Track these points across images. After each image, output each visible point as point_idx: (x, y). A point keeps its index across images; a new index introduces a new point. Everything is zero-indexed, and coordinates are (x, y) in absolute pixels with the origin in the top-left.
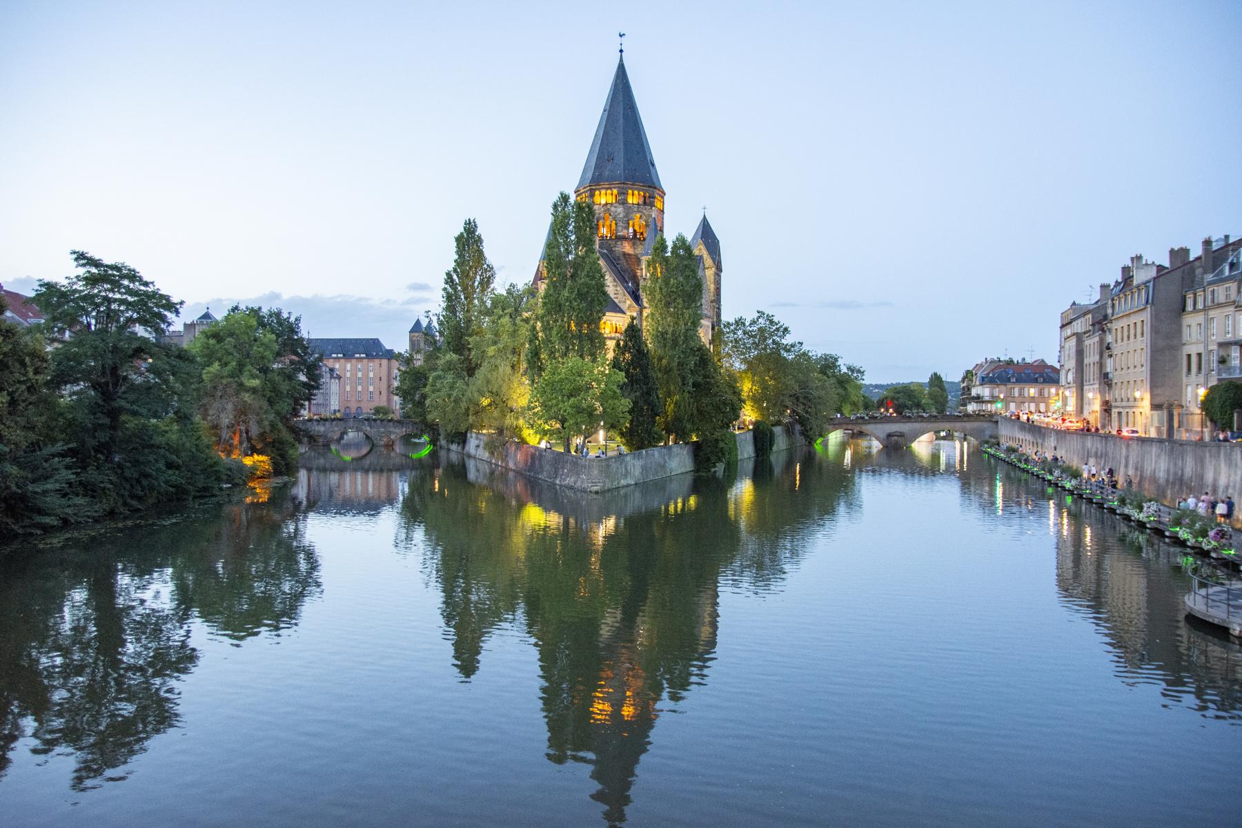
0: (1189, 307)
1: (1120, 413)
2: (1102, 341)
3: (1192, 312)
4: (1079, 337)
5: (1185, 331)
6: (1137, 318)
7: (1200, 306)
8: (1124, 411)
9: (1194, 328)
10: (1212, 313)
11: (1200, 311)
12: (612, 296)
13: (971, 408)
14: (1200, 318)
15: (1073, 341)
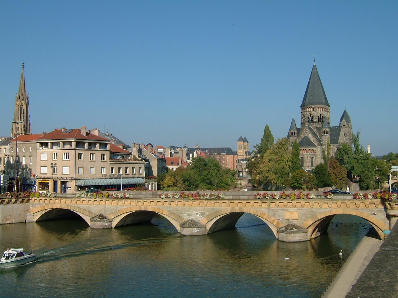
12: (312, 141)
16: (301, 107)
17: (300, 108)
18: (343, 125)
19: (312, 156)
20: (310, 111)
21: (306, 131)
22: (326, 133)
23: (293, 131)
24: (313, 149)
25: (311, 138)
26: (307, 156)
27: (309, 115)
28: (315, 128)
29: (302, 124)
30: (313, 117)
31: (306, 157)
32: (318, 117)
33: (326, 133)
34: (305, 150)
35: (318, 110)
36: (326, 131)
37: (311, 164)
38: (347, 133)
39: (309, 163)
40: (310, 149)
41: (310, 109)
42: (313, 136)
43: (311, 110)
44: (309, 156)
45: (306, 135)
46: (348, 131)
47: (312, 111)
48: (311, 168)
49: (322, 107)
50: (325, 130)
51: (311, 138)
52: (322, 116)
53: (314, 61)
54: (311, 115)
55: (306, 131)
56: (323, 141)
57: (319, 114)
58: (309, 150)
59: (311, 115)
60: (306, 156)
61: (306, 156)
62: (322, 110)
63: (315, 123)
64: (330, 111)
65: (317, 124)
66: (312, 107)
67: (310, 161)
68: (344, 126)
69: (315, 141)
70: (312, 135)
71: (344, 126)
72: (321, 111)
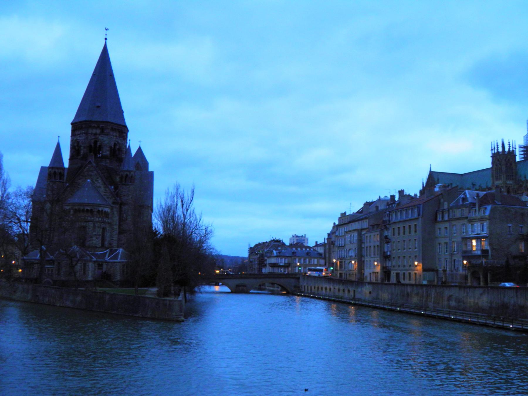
0: (439, 218)
1: (398, 274)
2: (381, 235)
3: (441, 222)
4: (360, 231)
5: (438, 232)
6: (413, 224)
7: (446, 218)
8: (401, 273)
9: (443, 229)
10: (454, 223)
11: (446, 221)
12: (102, 194)
13: (266, 270)
14: (447, 225)
15: (356, 234)
16: (72, 124)
17: (70, 126)
19: (103, 225)
20: (95, 134)
21: (90, 173)
23: (57, 171)
25: (100, 187)
26: (94, 224)
27: (93, 141)
29: (71, 159)
30: (100, 146)
31: (92, 225)
32: (111, 147)
34: (91, 210)
37: (100, 242)
39: (97, 238)
40: (100, 209)
41: (96, 128)
42: (105, 184)
43: (98, 131)
44: (97, 225)
48: (100, 249)
51: (100, 187)
52: (117, 147)
53: (106, 39)
54: (95, 143)
55: (90, 173)
56: (124, 196)
57: (113, 143)
58: (99, 210)
59: (95, 143)
60: (91, 225)
61: (91, 225)
62: (118, 135)
67: (99, 235)
70: (102, 180)
72: (116, 136)
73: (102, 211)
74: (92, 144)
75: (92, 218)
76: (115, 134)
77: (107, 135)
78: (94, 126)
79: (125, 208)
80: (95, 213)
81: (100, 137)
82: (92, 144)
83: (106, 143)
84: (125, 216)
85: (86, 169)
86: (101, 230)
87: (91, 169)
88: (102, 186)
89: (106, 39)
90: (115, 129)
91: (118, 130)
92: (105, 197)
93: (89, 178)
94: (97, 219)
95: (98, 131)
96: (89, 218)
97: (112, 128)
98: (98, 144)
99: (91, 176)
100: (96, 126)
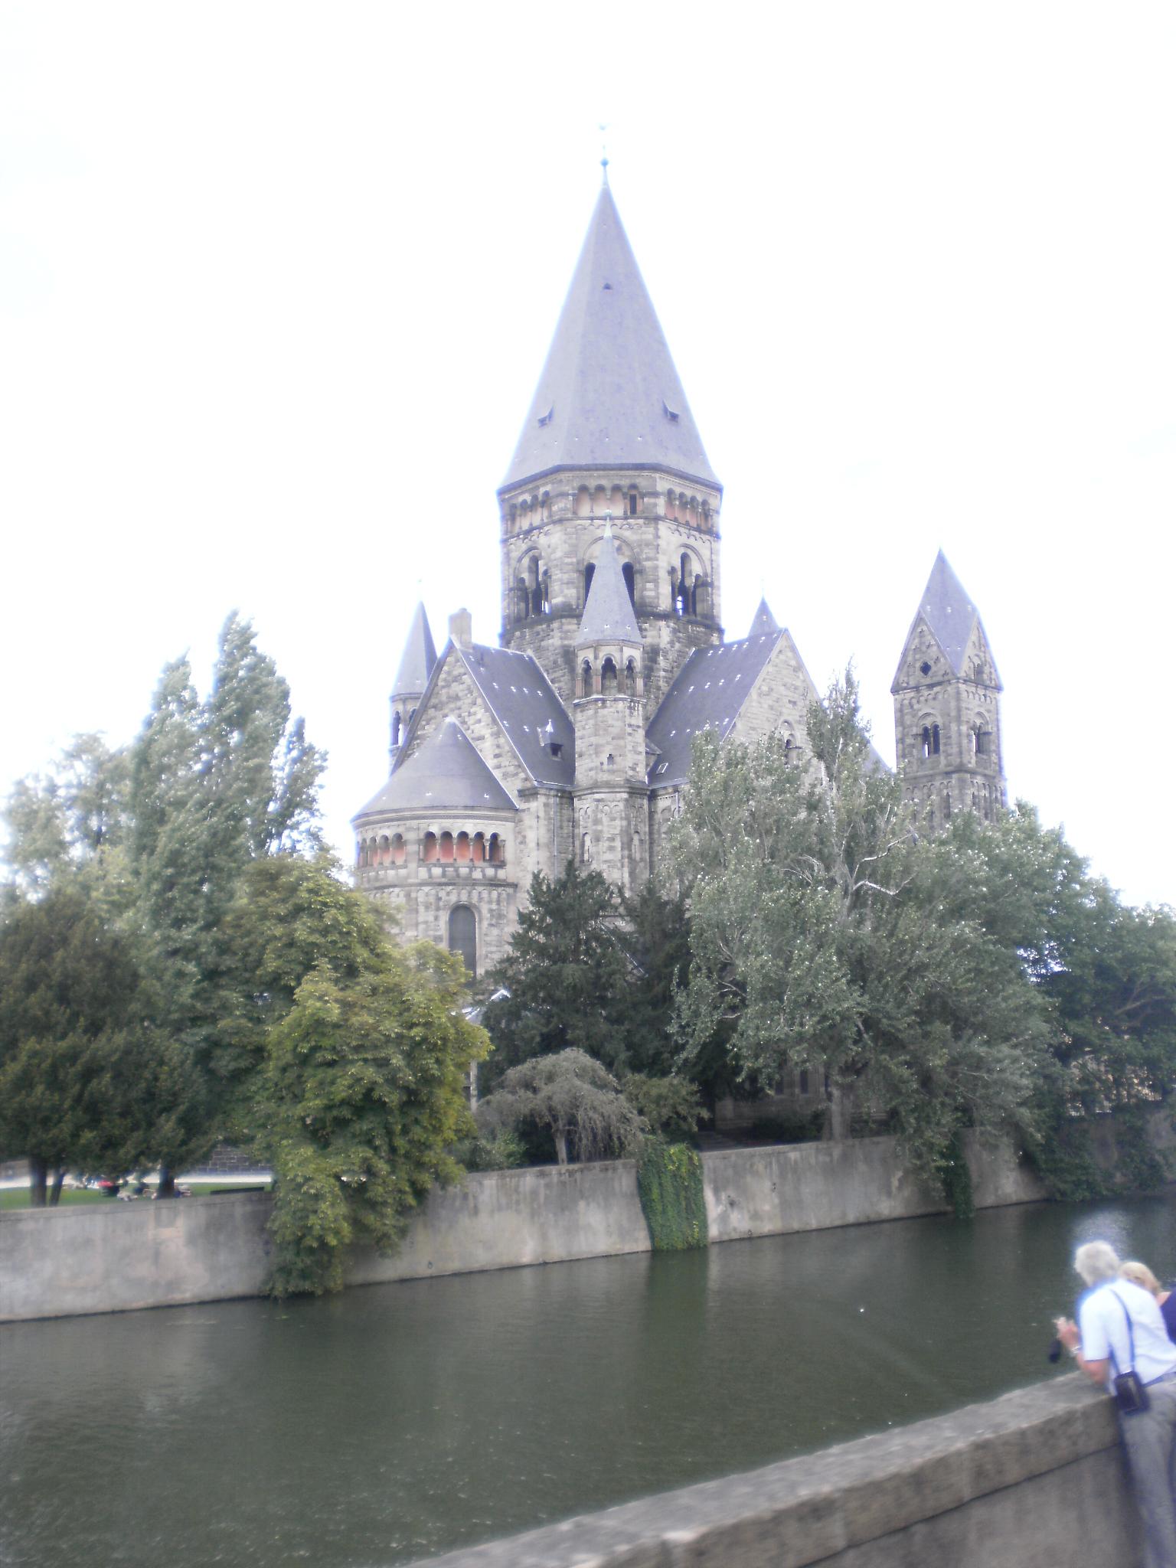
12: (490, 763)
18: (918, 665)
19: (453, 896)
21: (456, 688)
22: (596, 681)
24: (471, 828)
26: (408, 895)
27: (526, 561)
28: (560, 661)
30: (546, 573)
33: (596, 681)
34: (399, 837)
35: (585, 510)
36: (598, 665)
38: (947, 727)
42: (494, 721)
45: (451, 719)
46: (953, 704)
47: (539, 528)
49: (625, 483)
50: (591, 657)
51: (481, 738)
53: (605, 163)
62: (618, 509)
63: (555, 625)
64: (724, 522)
65: (570, 625)
66: (542, 490)
68: (926, 669)
69: (505, 761)
70: (487, 710)
71: (926, 669)
73: (447, 835)
74: (525, 576)
75: (403, 872)
76: (603, 510)
77: (561, 521)
78: (525, 502)
79: (584, 806)
80: (412, 848)
81: (542, 541)
82: (525, 576)
83: (559, 554)
84: (587, 839)
85: (443, 676)
86: (444, 917)
87: (456, 673)
88: (487, 732)
89: (605, 163)
90: (600, 489)
91: (616, 489)
92: (497, 774)
93: (452, 710)
94: (423, 873)
95: (537, 518)
96: (391, 873)
97: (583, 489)
98: (542, 569)
99: (457, 698)
100: (528, 497)
